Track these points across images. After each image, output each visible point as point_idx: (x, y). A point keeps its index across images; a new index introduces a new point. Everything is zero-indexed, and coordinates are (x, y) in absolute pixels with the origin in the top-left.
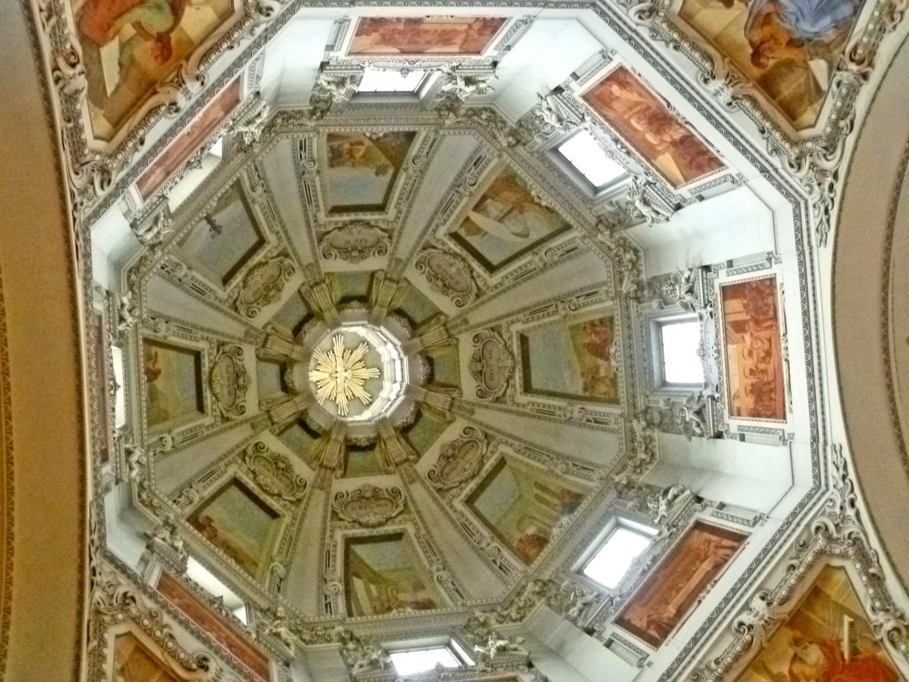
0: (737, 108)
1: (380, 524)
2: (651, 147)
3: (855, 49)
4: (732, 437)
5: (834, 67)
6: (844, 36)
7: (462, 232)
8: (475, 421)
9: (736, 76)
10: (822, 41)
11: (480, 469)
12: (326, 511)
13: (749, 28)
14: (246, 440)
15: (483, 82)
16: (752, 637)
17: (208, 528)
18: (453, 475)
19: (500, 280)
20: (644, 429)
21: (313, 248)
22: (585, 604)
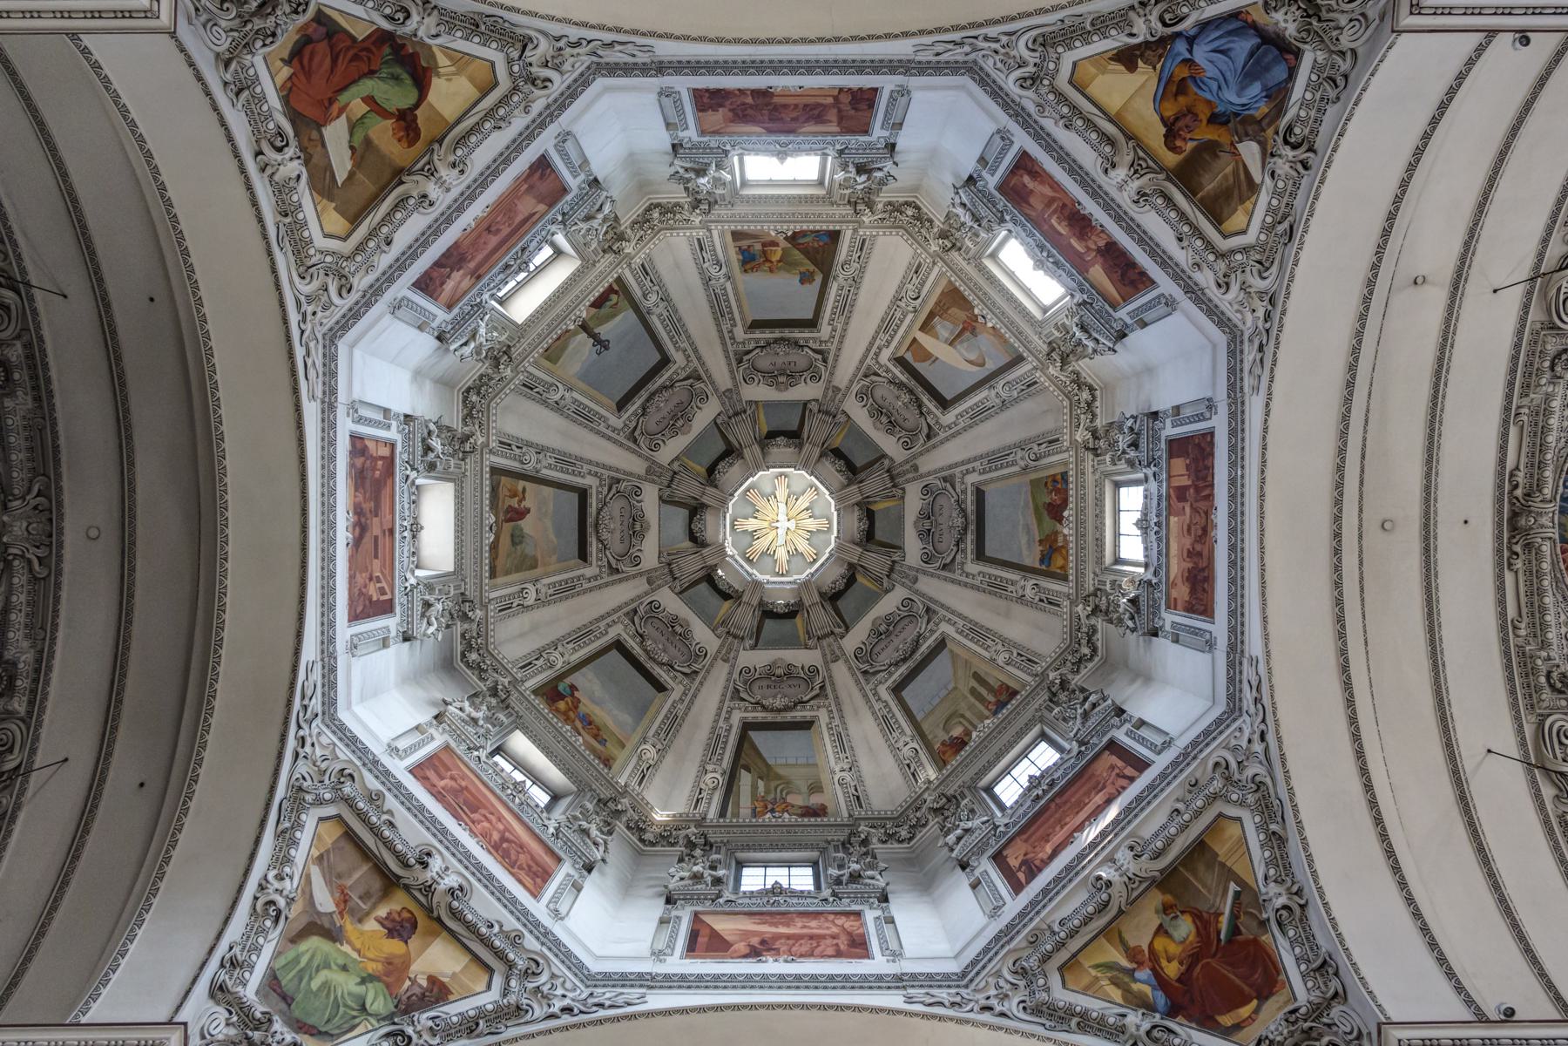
0: (1147, 207)
1: (786, 709)
2: (1080, 255)
3: (1290, 129)
4: (1165, 637)
5: (1267, 154)
6: (1280, 110)
7: (909, 357)
8: (916, 592)
9: (1144, 165)
10: (1251, 116)
11: (913, 652)
12: (726, 688)
13: (1160, 100)
14: (639, 597)
15: (880, 169)
16: (1110, 896)
17: (569, 700)
18: (881, 657)
19: (954, 419)
20: (1088, 617)
21: (732, 372)
22: (966, 831)
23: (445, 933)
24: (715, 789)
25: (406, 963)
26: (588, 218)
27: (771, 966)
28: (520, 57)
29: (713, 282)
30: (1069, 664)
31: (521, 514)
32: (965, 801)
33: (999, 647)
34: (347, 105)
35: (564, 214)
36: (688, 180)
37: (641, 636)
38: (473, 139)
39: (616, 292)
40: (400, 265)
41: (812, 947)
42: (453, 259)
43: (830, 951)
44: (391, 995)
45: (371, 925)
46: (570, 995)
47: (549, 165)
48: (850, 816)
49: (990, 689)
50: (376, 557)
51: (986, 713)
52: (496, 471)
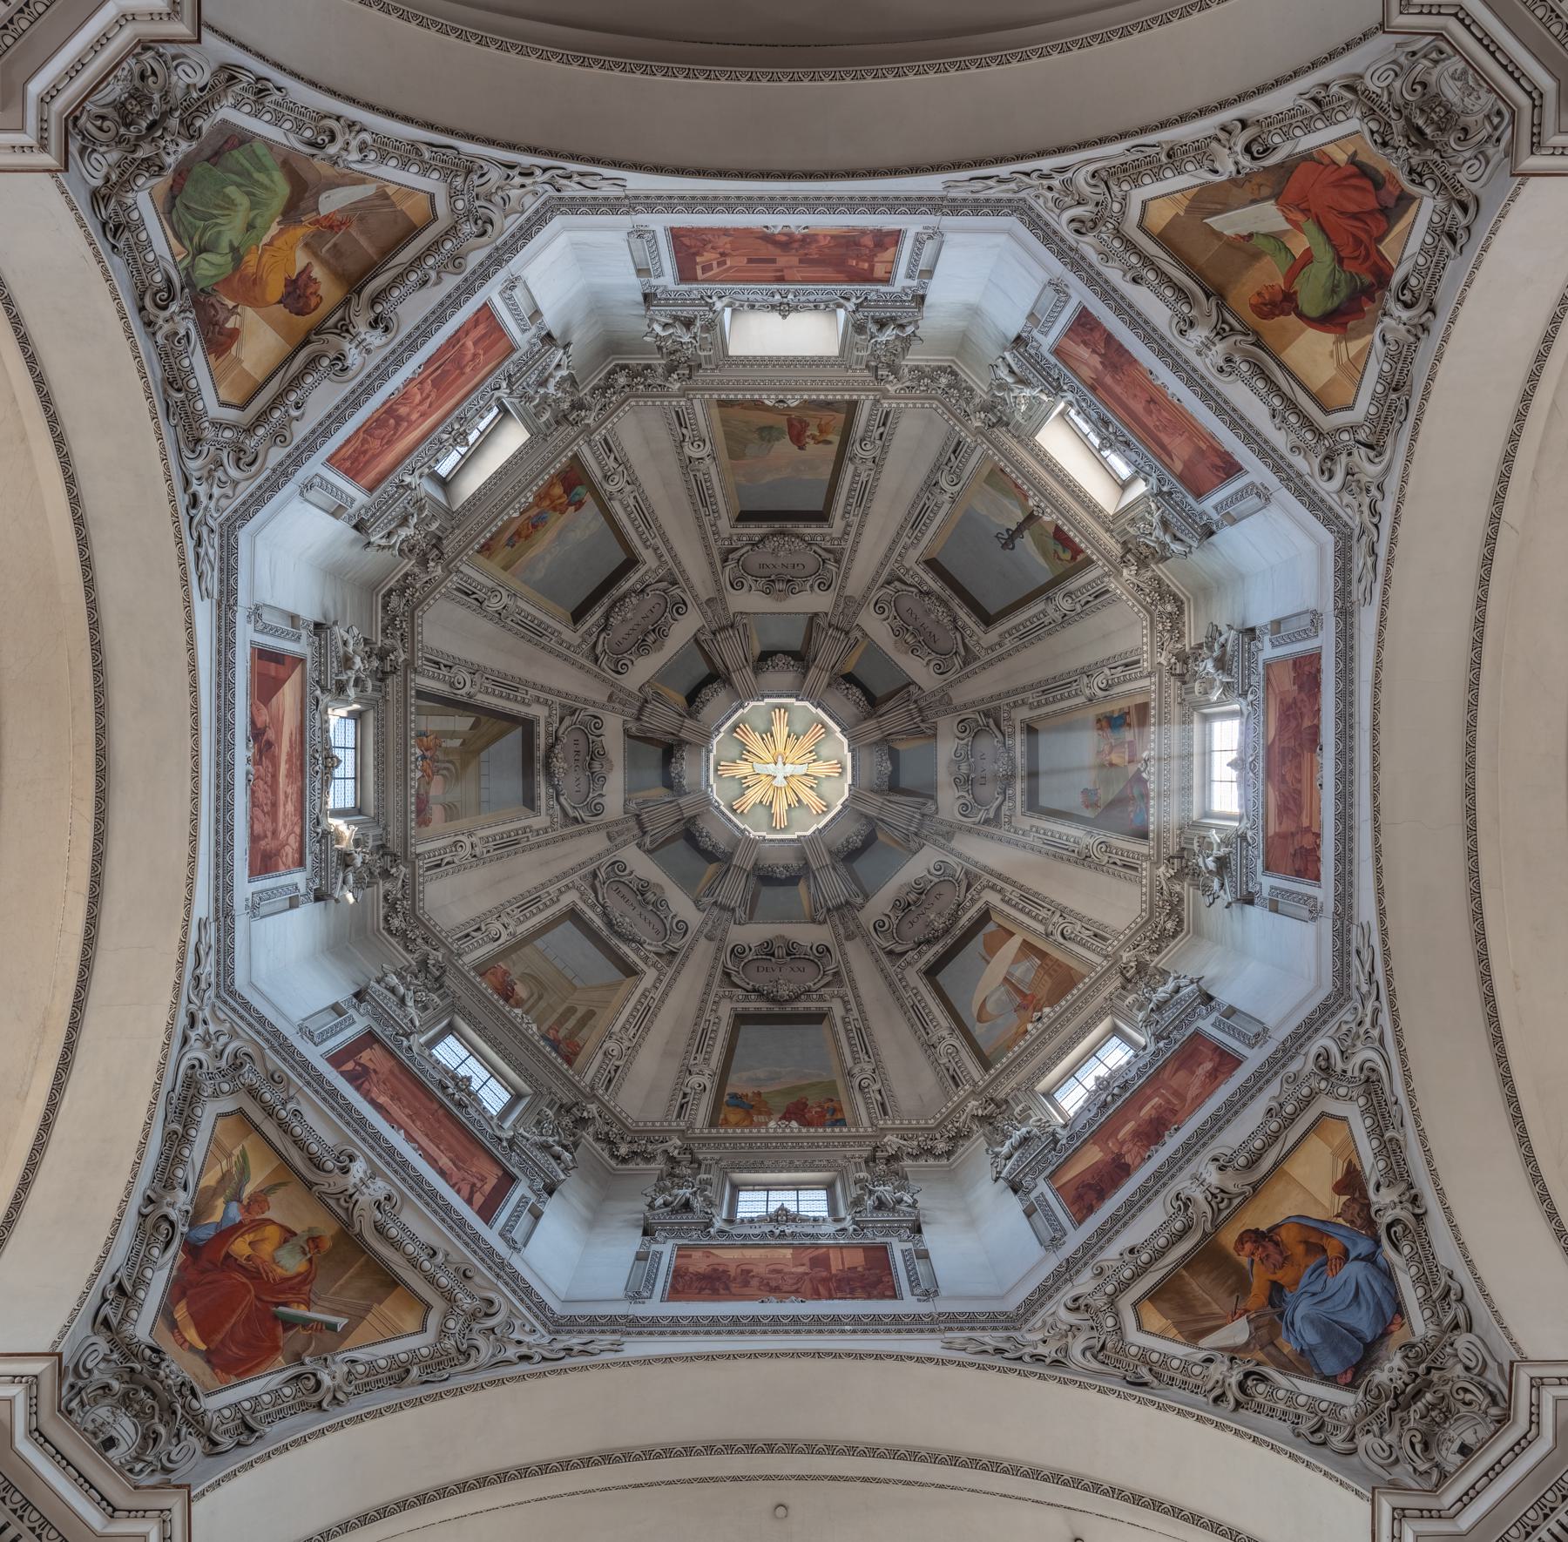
22: (402, 1001)
23: (289, 349)
25: (256, 302)
26: (1165, 524)
27: (242, 752)
28: (1359, 442)
29: (1086, 680)
30: (606, 1128)
31: (798, 439)
32: (437, 999)
33: (627, 1043)
34: (1301, 230)
35: (1170, 494)
36: (1211, 648)
37: (642, 591)
38: (1260, 384)
39: (1074, 558)
40: (1108, 293)
41: (266, 806)
42: (1115, 356)
43: (258, 828)
44: (217, 284)
45: (301, 259)
46: (212, 505)
47: (1229, 476)
48: (418, 855)
49: (573, 1033)
50: (750, 261)
51: (545, 1027)
52: (852, 406)
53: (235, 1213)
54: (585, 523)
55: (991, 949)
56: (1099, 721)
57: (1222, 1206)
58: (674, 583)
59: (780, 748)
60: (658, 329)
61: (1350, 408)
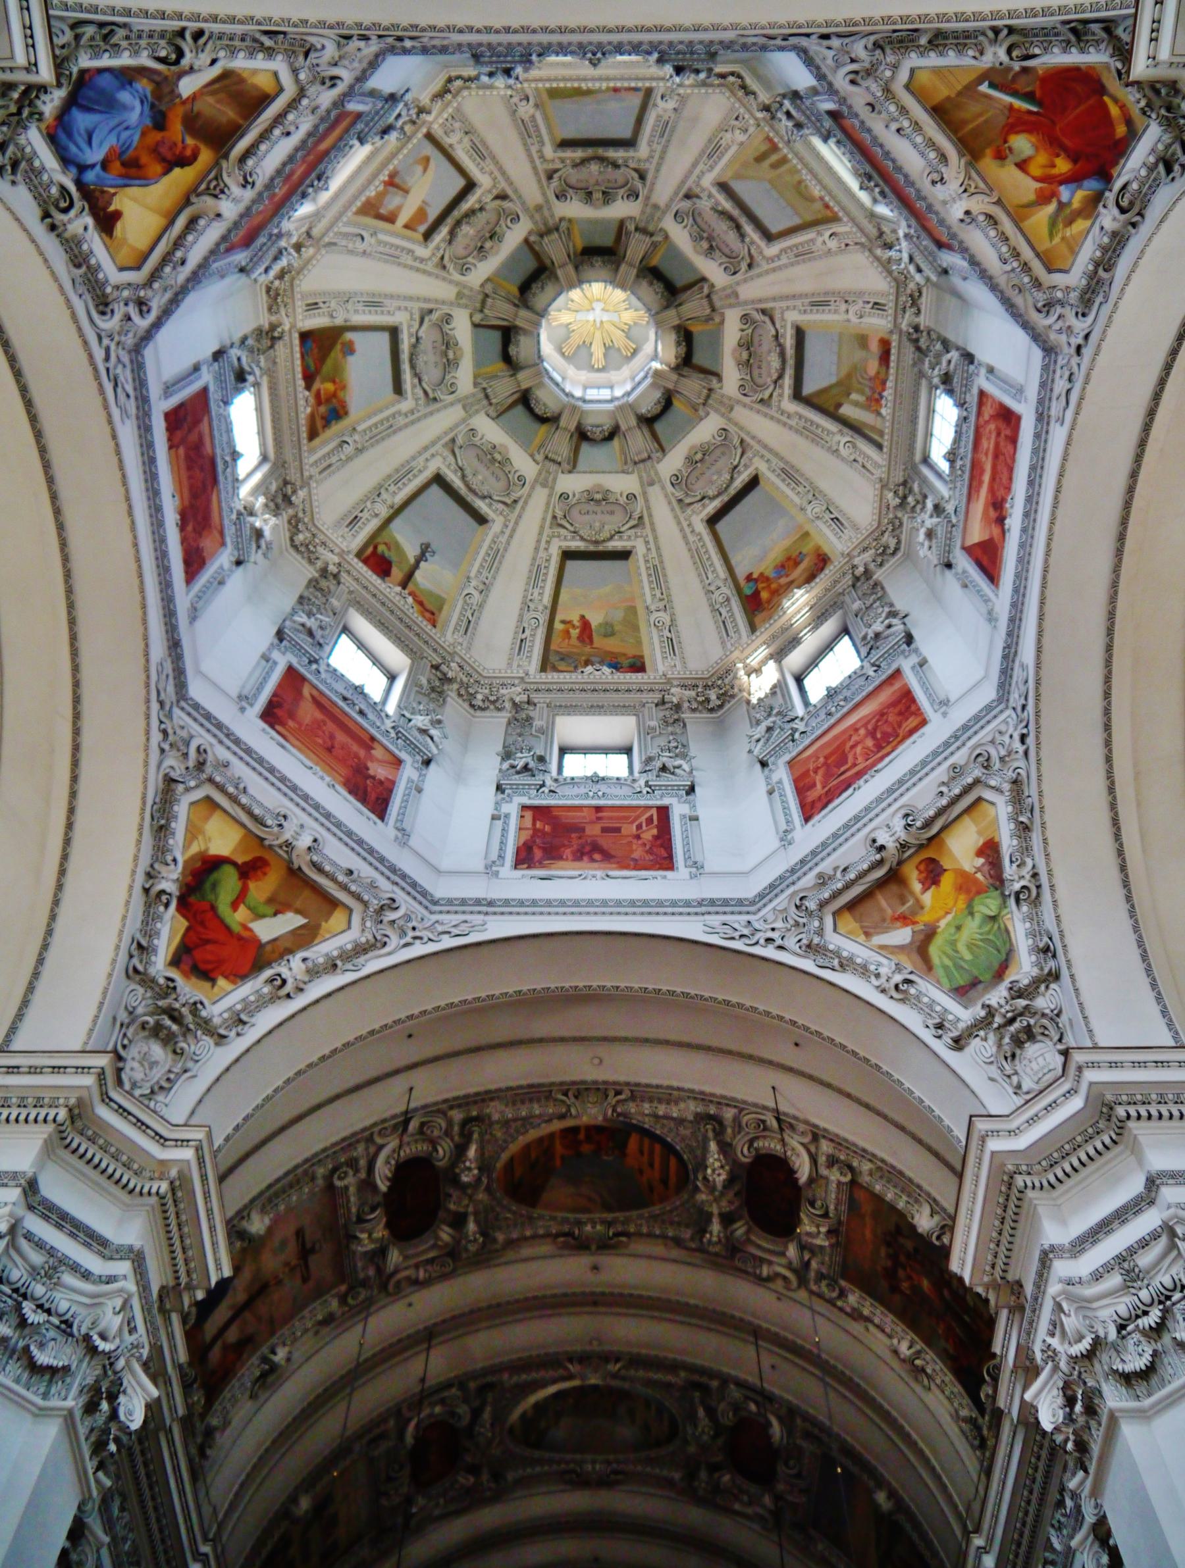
22: (911, 259)
24: (854, 446)
25: (962, 874)
31: (585, 625)
35: (310, 662)
38: (257, 811)
39: (375, 548)
43: (1010, 447)
45: (927, 898)
53: (1064, 192)
54: (747, 561)
55: (421, 214)
56: (346, 413)
57: (214, 183)
58: (680, 501)
59: (598, 334)
60: (686, 767)
61: (192, 804)
